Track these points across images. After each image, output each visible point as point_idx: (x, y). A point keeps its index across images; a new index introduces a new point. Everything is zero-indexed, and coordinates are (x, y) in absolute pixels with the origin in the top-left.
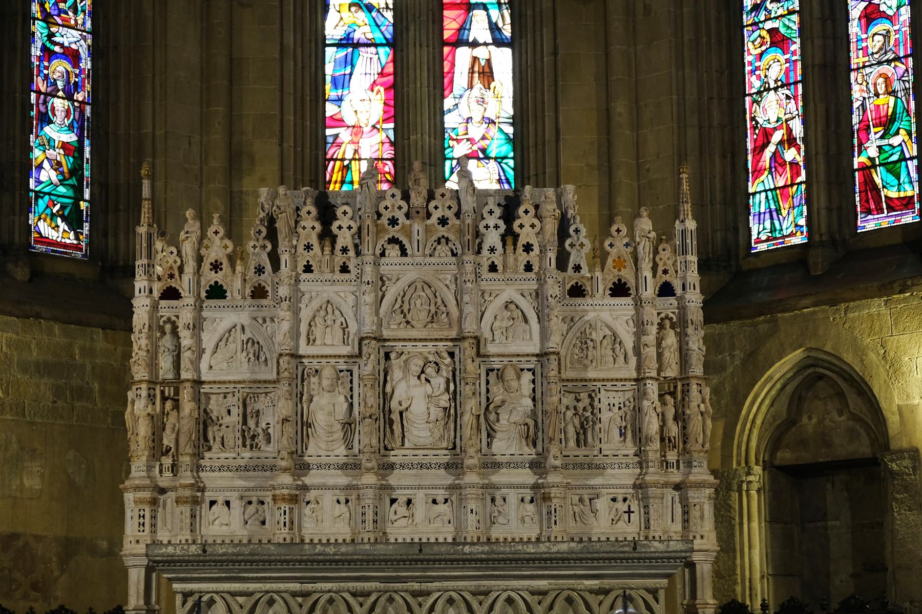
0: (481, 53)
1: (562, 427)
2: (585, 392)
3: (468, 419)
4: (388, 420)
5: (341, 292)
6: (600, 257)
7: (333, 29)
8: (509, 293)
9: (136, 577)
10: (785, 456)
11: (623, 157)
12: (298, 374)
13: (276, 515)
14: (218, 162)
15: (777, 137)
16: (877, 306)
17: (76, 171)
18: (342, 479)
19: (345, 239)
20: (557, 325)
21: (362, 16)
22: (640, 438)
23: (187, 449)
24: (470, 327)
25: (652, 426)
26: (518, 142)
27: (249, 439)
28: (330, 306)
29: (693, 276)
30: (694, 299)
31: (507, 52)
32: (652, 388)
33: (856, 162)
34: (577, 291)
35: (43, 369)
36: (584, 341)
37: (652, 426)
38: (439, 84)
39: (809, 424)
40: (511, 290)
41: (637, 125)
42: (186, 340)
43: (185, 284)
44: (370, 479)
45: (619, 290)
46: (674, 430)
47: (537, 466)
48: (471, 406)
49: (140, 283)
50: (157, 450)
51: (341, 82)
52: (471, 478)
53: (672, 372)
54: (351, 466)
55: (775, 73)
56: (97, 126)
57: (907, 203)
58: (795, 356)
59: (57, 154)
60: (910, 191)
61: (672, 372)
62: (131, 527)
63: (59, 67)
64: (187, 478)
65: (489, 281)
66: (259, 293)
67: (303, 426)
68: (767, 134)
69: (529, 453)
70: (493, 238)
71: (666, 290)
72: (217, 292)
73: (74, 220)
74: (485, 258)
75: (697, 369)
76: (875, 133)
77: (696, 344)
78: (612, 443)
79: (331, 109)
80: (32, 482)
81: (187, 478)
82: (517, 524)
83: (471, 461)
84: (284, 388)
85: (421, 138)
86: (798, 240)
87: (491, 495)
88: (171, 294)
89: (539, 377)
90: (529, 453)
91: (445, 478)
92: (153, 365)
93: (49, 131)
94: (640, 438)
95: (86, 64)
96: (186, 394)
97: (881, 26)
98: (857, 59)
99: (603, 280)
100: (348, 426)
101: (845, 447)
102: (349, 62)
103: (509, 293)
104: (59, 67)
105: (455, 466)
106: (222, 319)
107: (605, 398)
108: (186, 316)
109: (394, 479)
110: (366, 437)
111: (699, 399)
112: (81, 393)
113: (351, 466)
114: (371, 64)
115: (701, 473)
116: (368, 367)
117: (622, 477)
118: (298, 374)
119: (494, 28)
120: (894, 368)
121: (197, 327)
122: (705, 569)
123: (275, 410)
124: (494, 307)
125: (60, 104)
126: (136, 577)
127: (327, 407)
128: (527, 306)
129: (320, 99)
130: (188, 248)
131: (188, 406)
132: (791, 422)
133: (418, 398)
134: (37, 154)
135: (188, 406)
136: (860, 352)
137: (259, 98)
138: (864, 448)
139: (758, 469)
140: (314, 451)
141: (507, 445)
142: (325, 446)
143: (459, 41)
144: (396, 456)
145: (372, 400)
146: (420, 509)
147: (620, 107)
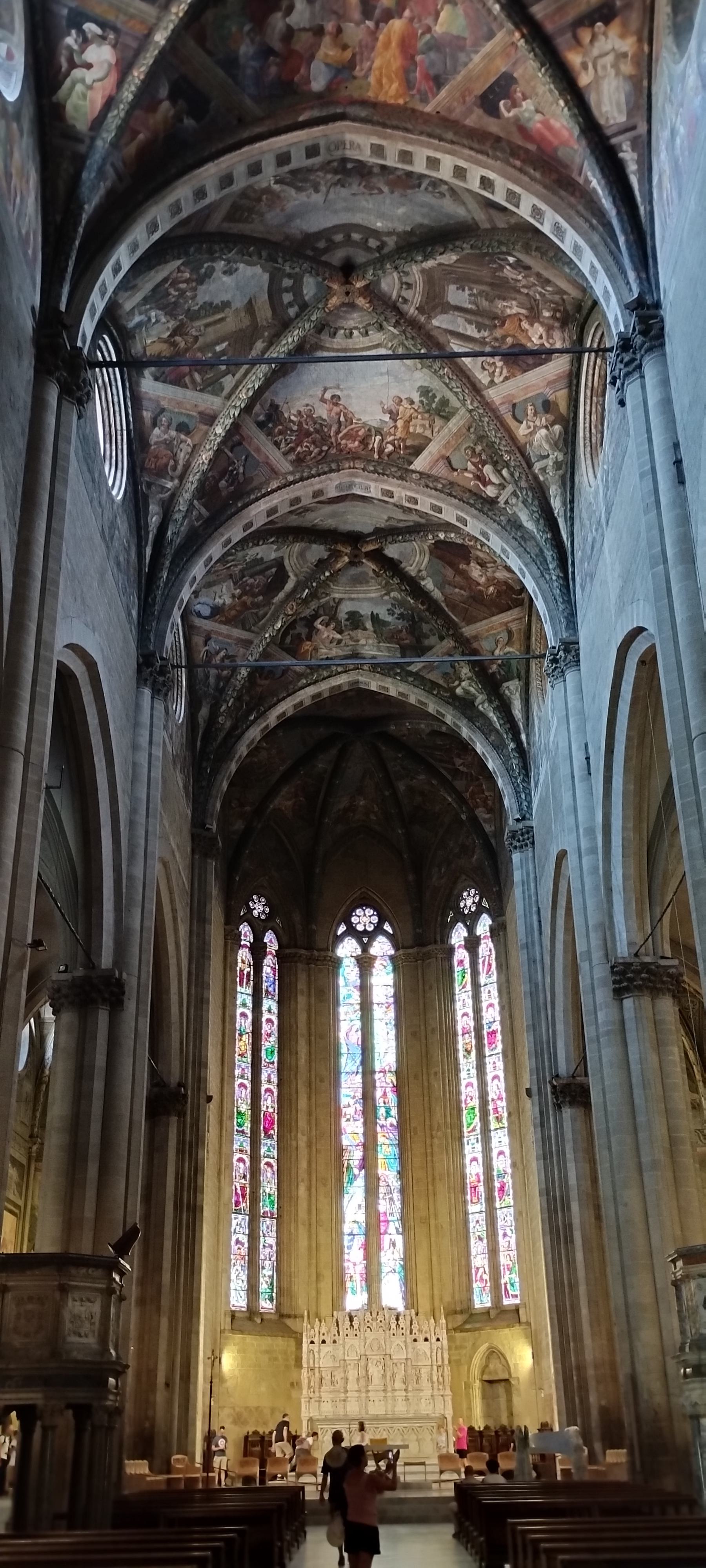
0: (393, 1237)
1: (412, 1380)
2: (418, 1369)
3: (388, 1378)
4: (368, 1378)
5: (356, 1342)
6: (420, 1331)
7: (346, 1228)
8: (398, 1342)
9: (305, 1423)
10: (486, 1377)
11: (436, 1275)
12: (344, 1365)
13: (340, 1405)
14: (314, 1278)
15: (481, 1270)
16: (507, 1331)
17: (272, 1284)
18: (357, 1395)
19: (356, 1327)
20: (410, 1350)
21: (356, 1225)
22: (432, 1382)
23: (317, 1386)
24: (388, 1352)
25: (435, 1379)
26: (404, 1267)
27: (332, 1383)
28: (352, 1346)
29: (445, 1336)
30: (445, 1342)
31: (400, 1237)
32: (435, 1368)
33: (503, 1281)
34: (415, 1340)
35: (267, 1352)
36: (417, 1355)
37: (435, 1379)
38: (379, 1248)
39: (491, 1366)
40: (399, 1341)
41: (440, 1264)
42: (317, 1356)
43: (316, 1340)
44: (364, 1395)
45: (426, 1340)
46: (441, 1379)
47: (406, 1390)
48: (389, 1374)
49: (304, 1340)
50: (309, 1388)
51: (349, 1248)
52: (389, 1394)
53: (440, 1363)
54: (359, 1391)
55: (480, 1249)
56: (278, 1269)
57: (516, 1296)
58: (486, 1345)
59: (267, 1279)
60: (518, 1293)
61: (440, 1363)
62: (303, 1409)
63: (268, 1250)
64: (317, 1394)
65: (393, 1338)
66: (335, 1342)
67: (346, 1379)
68: (478, 1269)
69: (404, 1387)
70: (393, 1326)
71: (438, 1340)
72: (324, 1342)
73: (271, 1299)
74: (392, 1332)
75: (446, 1362)
76: (508, 1272)
77: (446, 1356)
78: (425, 1383)
79: (346, 1257)
80: (263, 1389)
81: (317, 1394)
82: (401, 1408)
83: (389, 1389)
84: (341, 1369)
85: (374, 1267)
86: (489, 1305)
87: (394, 1398)
88: (312, 1342)
89: (406, 1365)
90: (404, 1387)
91: (383, 1394)
92: (308, 1363)
93: (264, 1272)
94: (432, 1382)
95: (275, 1248)
96: (317, 1370)
97: (507, 1239)
98: (501, 1249)
99: (421, 1338)
100: (358, 1379)
101: (503, 1376)
102: (352, 1240)
103: (398, 1342)
104: (268, 1250)
105: (385, 1391)
106: (325, 1349)
107: (423, 1371)
108: (316, 1350)
109: (370, 1394)
110: (362, 1382)
111: (447, 1371)
112: (276, 1359)
113: (359, 1391)
114: (360, 1240)
115: (448, 1392)
116: (363, 1363)
117: (427, 1393)
118: (344, 1365)
119: (397, 1229)
120: (512, 1352)
121: (319, 1352)
122: (449, 1419)
123: (339, 1375)
124: (395, 1345)
125: (267, 1262)
126: (305, 1423)
127: (352, 1374)
128: (403, 1345)
129: (342, 1253)
130: (317, 1330)
131: (317, 1374)
132: (487, 1366)
133: (375, 1371)
134: (261, 1280)
135: (317, 1374)
136: (503, 1345)
137: (325, 1257)
138: (506, 1376)
139: (478, 1381)
140: (349, 1387)
141: (398, 1385)
142: (352, 1386)
143: (386, 1233)
144: (370, 1388)
145: (364, 1372)
146: (377, 1402)
147: (434, 1259)
